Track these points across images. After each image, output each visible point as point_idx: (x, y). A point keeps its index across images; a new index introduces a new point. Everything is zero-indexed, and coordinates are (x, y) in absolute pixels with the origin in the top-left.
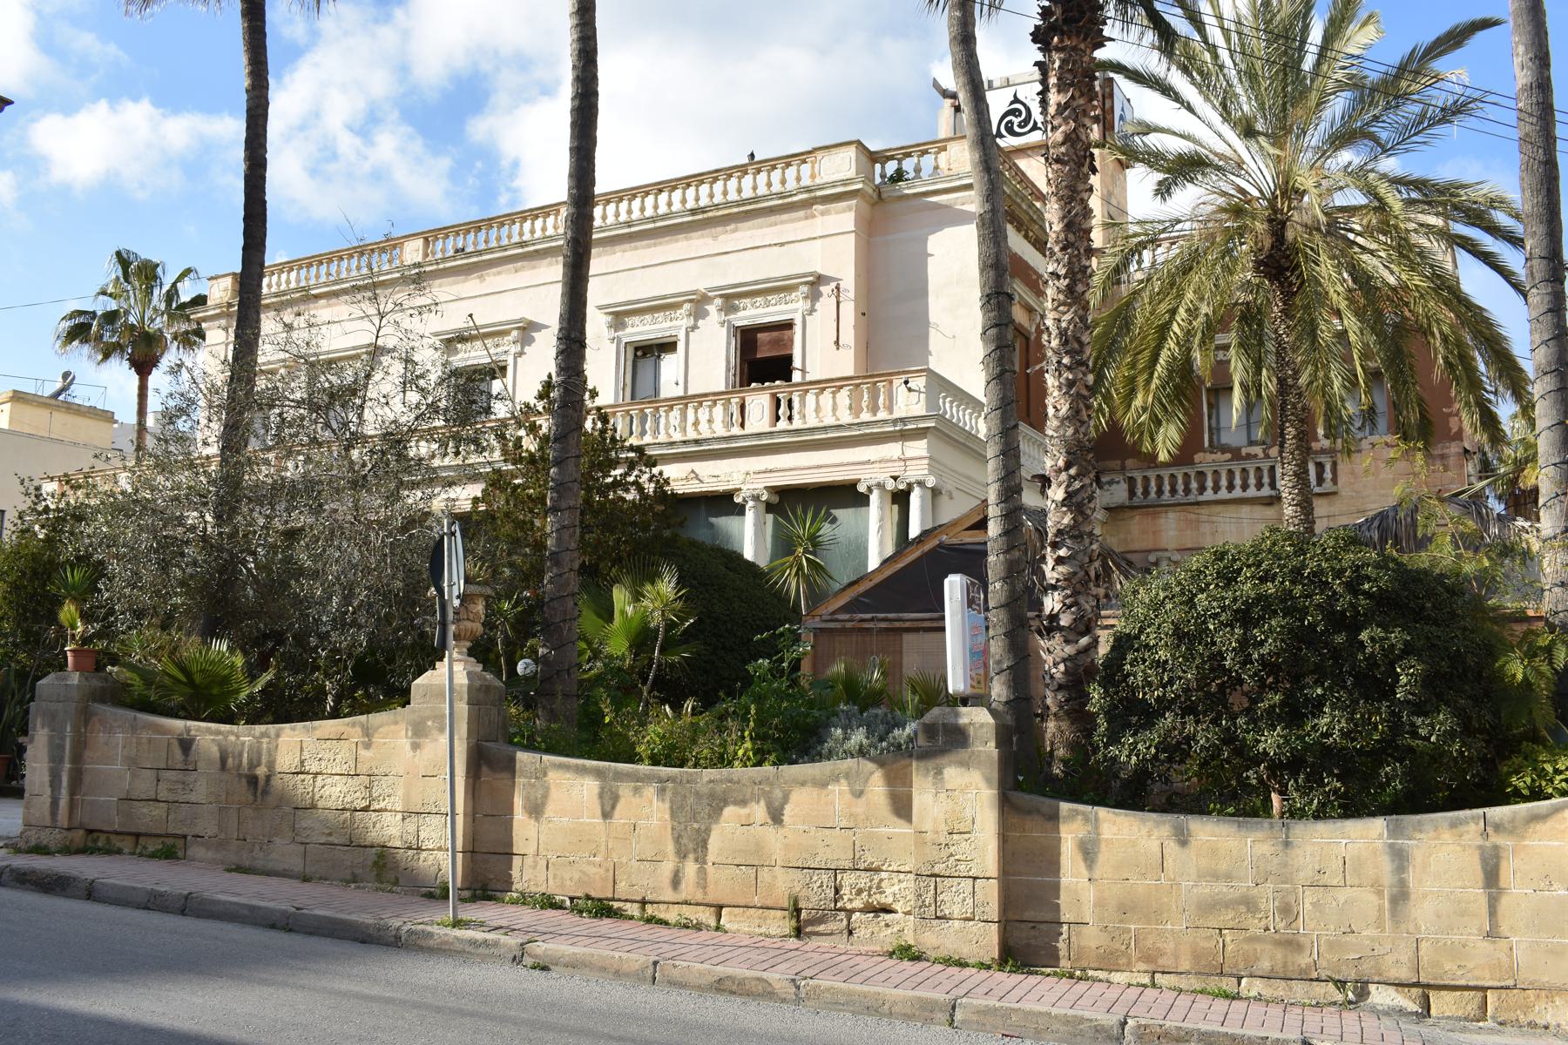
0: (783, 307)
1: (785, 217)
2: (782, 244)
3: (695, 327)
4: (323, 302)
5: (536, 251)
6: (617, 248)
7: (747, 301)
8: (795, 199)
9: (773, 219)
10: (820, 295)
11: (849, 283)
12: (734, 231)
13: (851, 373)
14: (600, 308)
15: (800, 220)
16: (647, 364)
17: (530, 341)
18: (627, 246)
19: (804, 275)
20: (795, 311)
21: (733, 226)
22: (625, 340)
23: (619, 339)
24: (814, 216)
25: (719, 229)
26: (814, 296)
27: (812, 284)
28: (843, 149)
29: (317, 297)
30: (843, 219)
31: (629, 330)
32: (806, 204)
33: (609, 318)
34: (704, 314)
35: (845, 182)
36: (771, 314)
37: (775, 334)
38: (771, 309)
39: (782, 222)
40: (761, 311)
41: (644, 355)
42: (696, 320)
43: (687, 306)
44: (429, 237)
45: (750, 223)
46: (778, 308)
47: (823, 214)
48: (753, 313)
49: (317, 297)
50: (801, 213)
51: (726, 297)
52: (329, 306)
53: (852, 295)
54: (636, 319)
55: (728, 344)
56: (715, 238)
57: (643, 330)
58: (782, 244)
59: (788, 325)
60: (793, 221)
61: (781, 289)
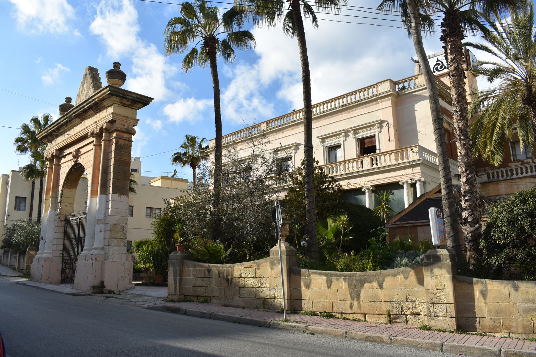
0: (372, 131)
1: (370, 104)
2: (370, 113)
3: (346, 140)
4: (240, 144)
7: (361, 130)
9: (366, 105)
10: (383, 126)
11: (391, 122)
13: (394, 148)
14: (317, 137)
15: (374, 105)
16: (332, 153)
20: (376, 132)
23: (324, 146)
26: (381, 127)
27: (380, 123)
29: (238, 143)
30: (388, 103)
31: (326, 143)
35: (387, 92)
37: (370, 139)
40: (365, 133)
43: (343, 134)
44: (267, 122)
47: (381, 102)
48: (363, 134)
49: (238, 143)
50: (375, 103)
51: (354, 130)
53: (392, 125)
54: (328, 139)
55: (356, 144)
56: (349, 113)
57: (330, 142)
58: (370, 113)
59: (374, 136)
60: (372, 105)
61: (370, 126)
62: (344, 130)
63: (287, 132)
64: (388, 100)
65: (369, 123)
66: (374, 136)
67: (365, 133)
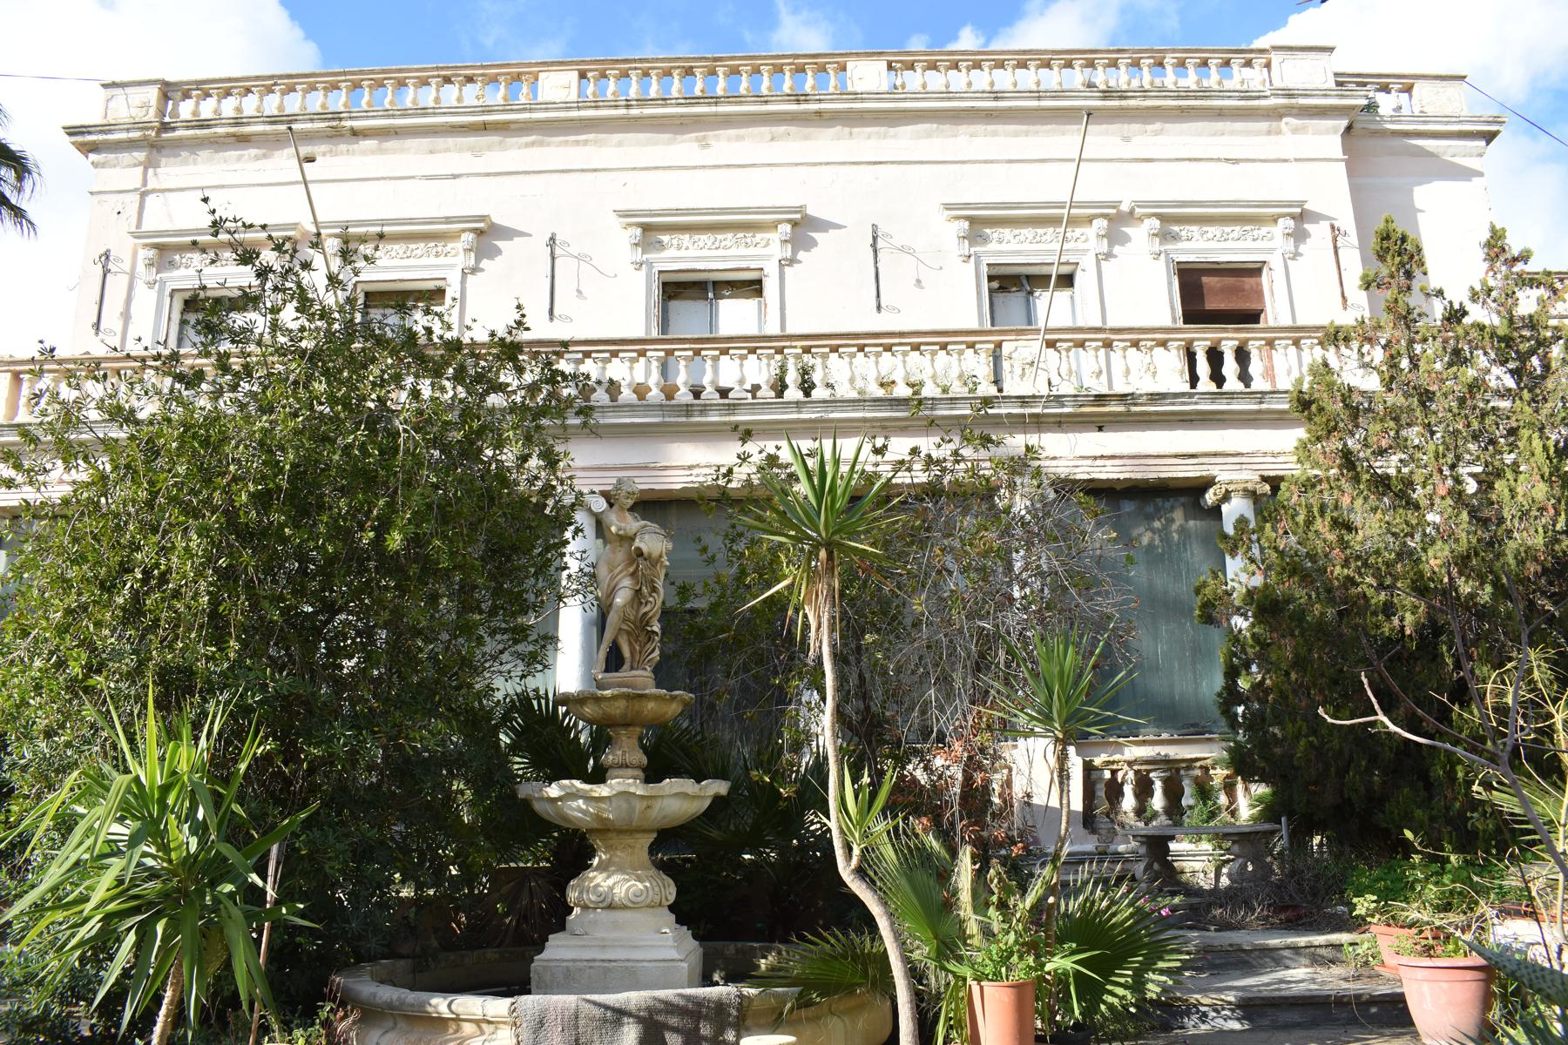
1: (1239, 126)
2: (1236, 161)
5: (819, 113)
6: (964, 128)
7: (1194, 228)
8: (1263, 103)
9: (1220, 125)
11: (1347, 221)
12: (1156, 133)
13: (639, 333)
15: (1258, 133)
16: (1014, 300)
17: (810, 244)
18: (980, 128)
19: (1290, 204)
20: (1271, 251)
21: (1157, 126)
24: (1279, 132)
25: (1136, 127)
26: (1299, 236)
27: (480, 233)
28: (1313, 55)
29: (355, 133)
30: (1327, 139)
31: (992, 246)
32: (1276, 114)
34: (1125, 239)
37: (1230, 280)
39: (1232, 133)
40: (1213, 245)
41: (1002, 289)
42: (1111, 245)
43: (1100, 224)
45: (1185, 126)
46: (1240, 244)
47: (1295, 131)
48: (1202, 246)
50: (1263, 125)
52: (382, 151)
53: (1353, 238)
54: (1007, 232)
55: (1170, 284)
56: (1127, 139)
58: (1236, 161)
59: (1255, 271)
60: (1248, 133)
62: (1115, 205)
63: (726, 146)
64: (1327, 132)
65: (1249, 204)
66: (1255, 271)
67: (1213, 245)
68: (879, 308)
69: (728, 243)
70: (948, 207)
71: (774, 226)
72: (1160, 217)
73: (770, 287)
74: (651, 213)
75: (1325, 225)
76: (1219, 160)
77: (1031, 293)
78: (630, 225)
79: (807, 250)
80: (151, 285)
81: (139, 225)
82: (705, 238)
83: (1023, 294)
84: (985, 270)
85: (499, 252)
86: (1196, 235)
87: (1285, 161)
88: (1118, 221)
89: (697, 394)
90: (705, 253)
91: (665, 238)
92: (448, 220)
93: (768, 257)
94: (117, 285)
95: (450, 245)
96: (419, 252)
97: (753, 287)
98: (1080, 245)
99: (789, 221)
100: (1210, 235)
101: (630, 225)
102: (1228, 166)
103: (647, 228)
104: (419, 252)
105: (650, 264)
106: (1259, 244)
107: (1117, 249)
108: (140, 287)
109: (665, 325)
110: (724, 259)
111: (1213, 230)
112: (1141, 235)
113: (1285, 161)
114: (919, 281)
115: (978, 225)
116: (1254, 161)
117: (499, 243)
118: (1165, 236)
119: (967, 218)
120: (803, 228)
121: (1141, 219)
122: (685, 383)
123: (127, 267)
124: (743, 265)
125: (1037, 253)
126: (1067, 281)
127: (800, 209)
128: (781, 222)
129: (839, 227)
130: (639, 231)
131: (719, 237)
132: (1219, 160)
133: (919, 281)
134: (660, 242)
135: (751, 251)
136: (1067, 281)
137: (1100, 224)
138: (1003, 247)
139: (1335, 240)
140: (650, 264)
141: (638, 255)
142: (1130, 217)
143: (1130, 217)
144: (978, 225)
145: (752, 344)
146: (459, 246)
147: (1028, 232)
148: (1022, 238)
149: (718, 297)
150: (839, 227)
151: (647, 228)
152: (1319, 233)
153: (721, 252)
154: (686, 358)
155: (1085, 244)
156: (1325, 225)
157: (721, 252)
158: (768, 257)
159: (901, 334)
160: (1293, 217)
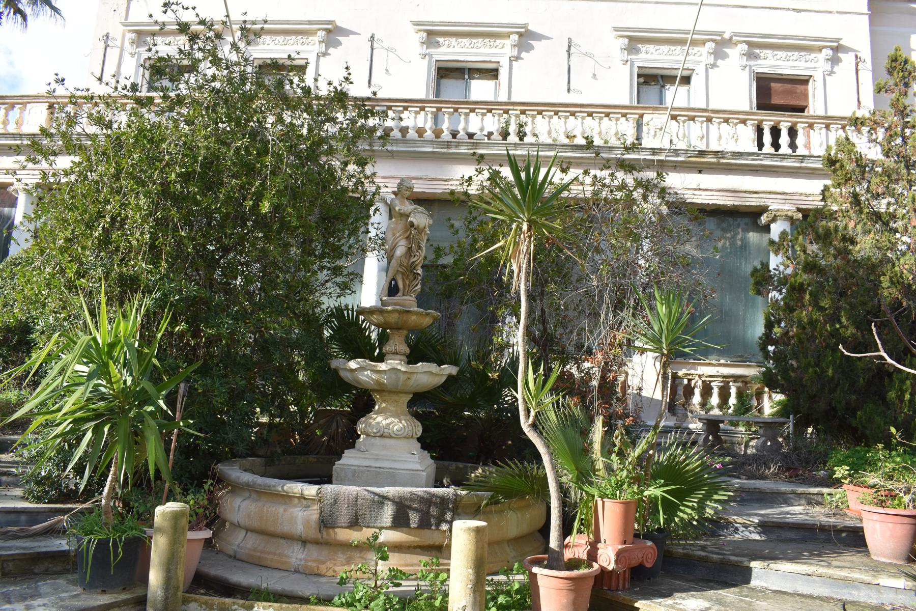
0: (803, 64)
2: (800, 11)
7: (769, 52)
11: (866, 53)
16: (653, 90)
17: (530, 48)
20: (816, 69)
22: (637, 64)
26: (835, 61)
33: (133, 36)
34: (725, 56)
36: (791, 67)
38: (791, 63)
40: (780, 63)
41: (646, 83)
42: (716, 59)
43: (710, 46)
46: (797, 64)
48: (774, 63)
53: (869, 64)
54: (651, 48)
55: (751, 86)
58: (800, 11)
59: (804, 81)
62: (720, 34)
66: (804, 81)
67: (780, 63)
68: (569, 90)
69: (479, 45)
70: (616, 29)
71: (507, 36)
72: (747, 43)
73: (503, 73)
74: (433, 24)
75: (852, 55)
76: (788, 9)
77: (663, 86)
78: (420, 30)
79: (528, 51)
80: (132, 55)
81: (126, 18)
82: (465, 41)
83: (658, 87)
84: (636, 70)
85: (340, 44)
86: (770, 56)
87: (831, 12)
88: (721, 44)
89: (454, 135)
90: (465, 50)
91: (441, 40)
92: (310, 23)
93: (502, 55)
94: (113, 55)
95: (311, 38)
96: (292, 42)
97: (492, 73)
98: (696, 58)
99: (517, 33)
100: (779, 57)
101: (420, 30)
102: (794, 13)
103: (430, 33)
104: (292, 42)
105: (431, 56)
106: (809, 64)
107: (719, 62)
108: (127, 57)
109: (438, 93)
110: (476, 54)
111: (781, 54)
112: (735, 54)
113: (831, 12)
114: (594, 75)
115: (635, 41)
116: (810, 11)
117: (340, 38)
118: (750, 55)
119: (627, 37)
120: (526, 38)
121: (736, 44)
122: (448, 129)
123: (119, 43)
124: (488, 59)
125: (669, 61)
126: (686, 80)
127: (525, 26)
128: (512, 33)
129: (548, 38)
130: (425, 34)
131: (474, 41)
132: (788, 9)
133: (594, 75)
134: (438, 42)
135: (493, 50)
136: (686, 80)
137: (710, 46)
138: (649, 56)
139: (857, 65)
140: (431, 56)
141: (424, 50)
142: (729, 42)
143: (729, 42)
144: (635, 41)
145: (490, 107)
146: (316, 39)
147: (664, 48)
148: (661, 51)
149: (471, 78)
150: (548, 38)
151: (430, 33)
152: (847, 59)
153: (474, 50)
154: (449, 113)
155: (700, 57)
156: (852, 55)
157: (474, 50)
158: (502, 55)
159: (582, 106)
160: (832, 48)
